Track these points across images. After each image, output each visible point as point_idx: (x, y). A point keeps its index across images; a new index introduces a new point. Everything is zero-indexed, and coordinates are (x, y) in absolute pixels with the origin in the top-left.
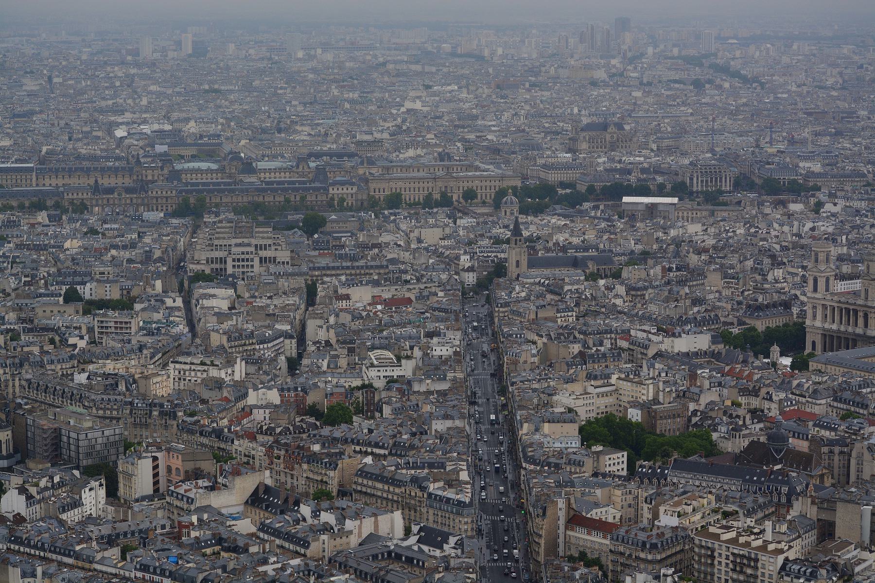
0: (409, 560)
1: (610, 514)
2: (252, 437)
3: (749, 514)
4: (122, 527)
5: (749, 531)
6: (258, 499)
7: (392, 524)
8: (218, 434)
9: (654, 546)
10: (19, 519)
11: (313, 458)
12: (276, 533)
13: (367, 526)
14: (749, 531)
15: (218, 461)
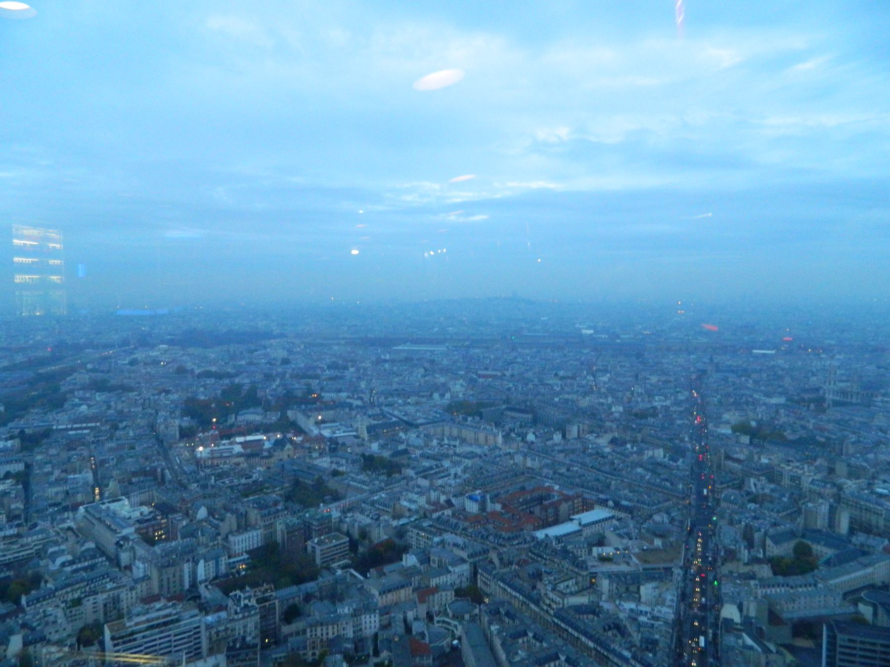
0: (665, 466)
1: (742, 457)
2: (612, 421)
3: (798, 461)
4: (566, 447)
5: (798, 467)
6: (613, 441)
7: (659, 453)
8: (601, 420)
9: (758, 470)
10: (532, 443)
11: (633, 429)
12: (618, 453)
13: (650, 453)
14: (798, 467)
15: (599, 428)
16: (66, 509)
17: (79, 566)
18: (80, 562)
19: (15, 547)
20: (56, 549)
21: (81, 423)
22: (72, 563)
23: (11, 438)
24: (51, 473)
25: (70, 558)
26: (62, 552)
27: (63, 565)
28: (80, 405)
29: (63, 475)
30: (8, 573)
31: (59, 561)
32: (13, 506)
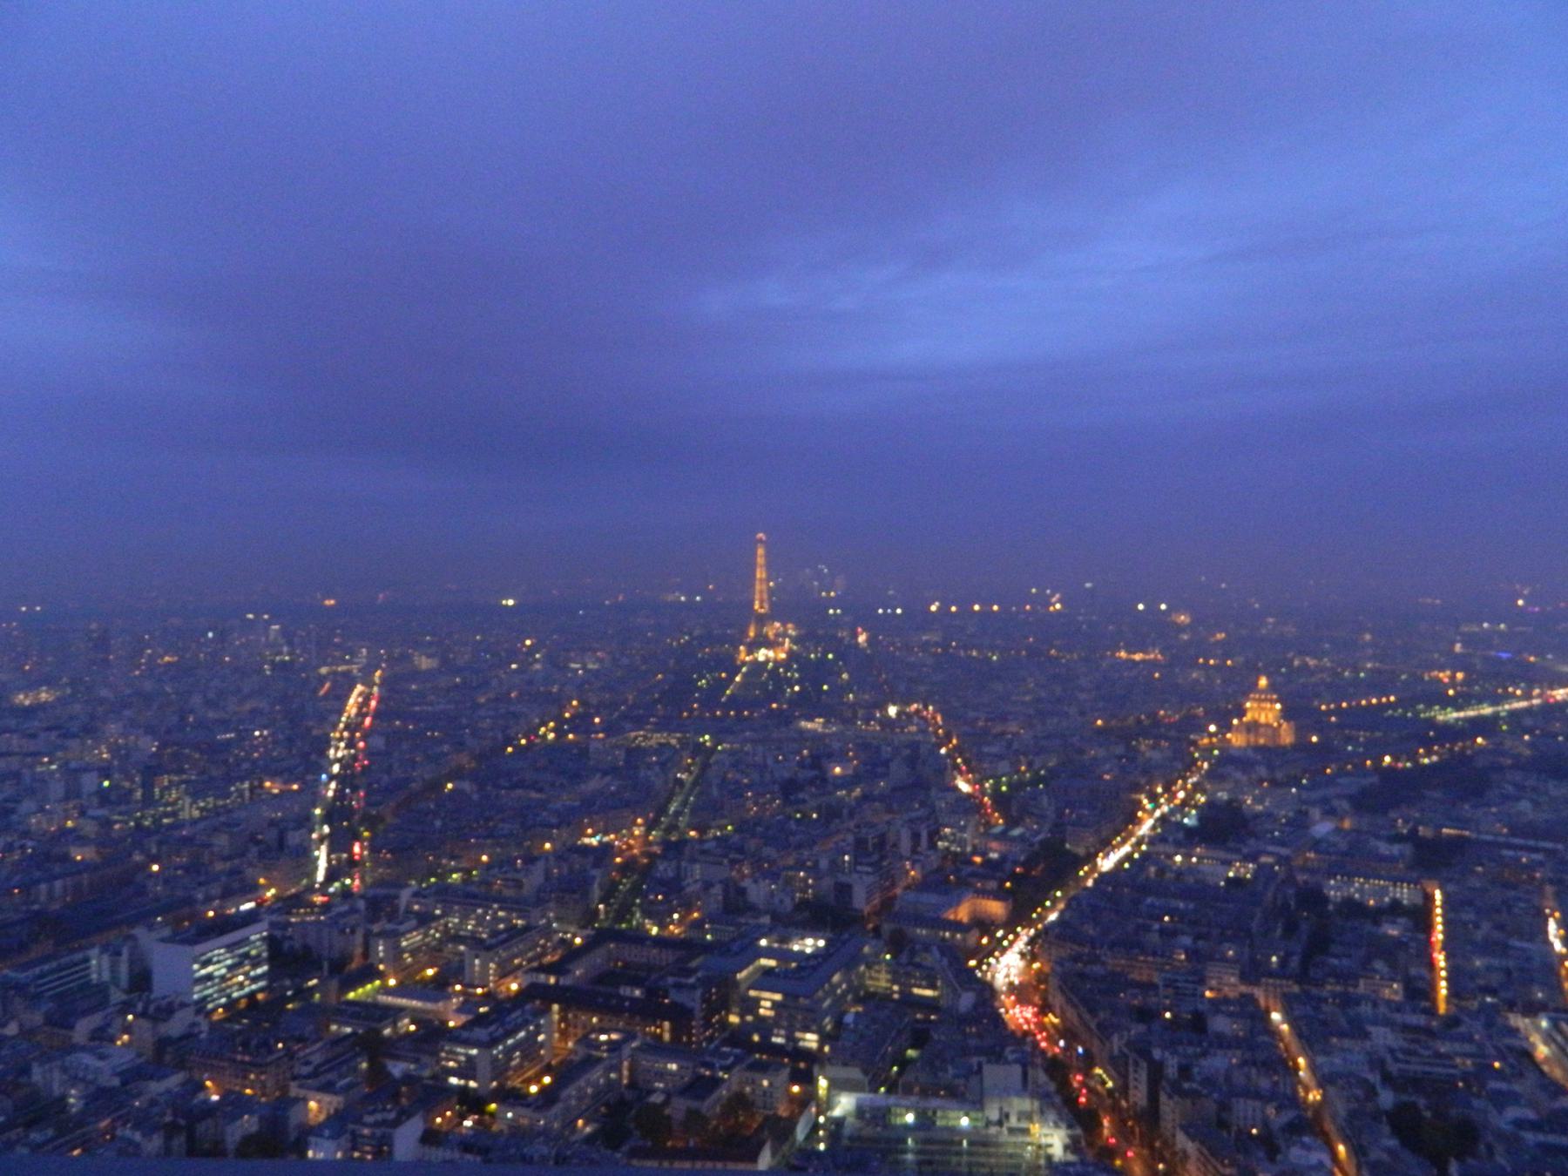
16: (1511, 1006)
17: (1552, 1139)
18: (1552, 1131)
19: (1427, 1053)
20: (1502, 1086)
21: (1525, 835)
22: (1535, 1126)
23: (1397, 838)
24: (1477, 926)
25: (1530, 1114)
26: (1514, 1098)
27: (1519, 1124)
28: (1518, 799)
29: (1497, 935)
30: (1413, 1098)
31: (1512, 1113)
32: (1413, 971)
